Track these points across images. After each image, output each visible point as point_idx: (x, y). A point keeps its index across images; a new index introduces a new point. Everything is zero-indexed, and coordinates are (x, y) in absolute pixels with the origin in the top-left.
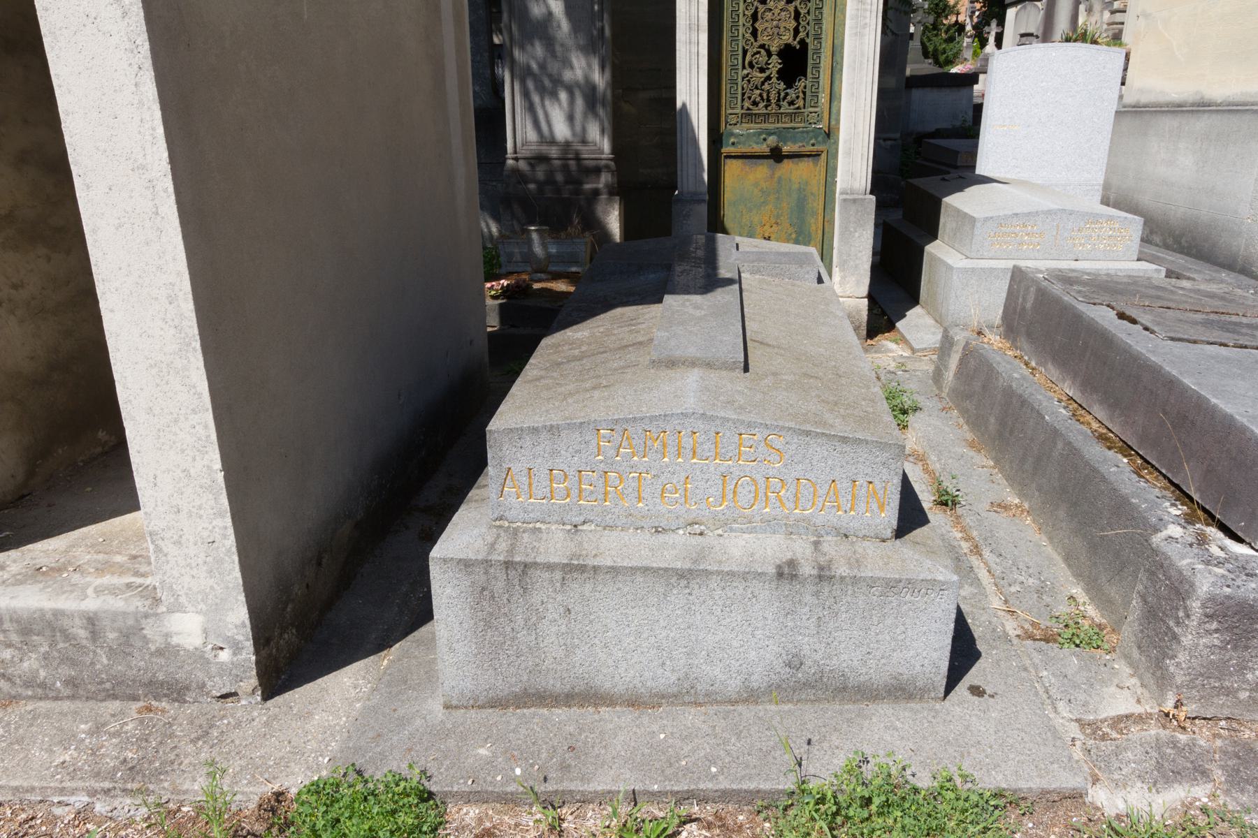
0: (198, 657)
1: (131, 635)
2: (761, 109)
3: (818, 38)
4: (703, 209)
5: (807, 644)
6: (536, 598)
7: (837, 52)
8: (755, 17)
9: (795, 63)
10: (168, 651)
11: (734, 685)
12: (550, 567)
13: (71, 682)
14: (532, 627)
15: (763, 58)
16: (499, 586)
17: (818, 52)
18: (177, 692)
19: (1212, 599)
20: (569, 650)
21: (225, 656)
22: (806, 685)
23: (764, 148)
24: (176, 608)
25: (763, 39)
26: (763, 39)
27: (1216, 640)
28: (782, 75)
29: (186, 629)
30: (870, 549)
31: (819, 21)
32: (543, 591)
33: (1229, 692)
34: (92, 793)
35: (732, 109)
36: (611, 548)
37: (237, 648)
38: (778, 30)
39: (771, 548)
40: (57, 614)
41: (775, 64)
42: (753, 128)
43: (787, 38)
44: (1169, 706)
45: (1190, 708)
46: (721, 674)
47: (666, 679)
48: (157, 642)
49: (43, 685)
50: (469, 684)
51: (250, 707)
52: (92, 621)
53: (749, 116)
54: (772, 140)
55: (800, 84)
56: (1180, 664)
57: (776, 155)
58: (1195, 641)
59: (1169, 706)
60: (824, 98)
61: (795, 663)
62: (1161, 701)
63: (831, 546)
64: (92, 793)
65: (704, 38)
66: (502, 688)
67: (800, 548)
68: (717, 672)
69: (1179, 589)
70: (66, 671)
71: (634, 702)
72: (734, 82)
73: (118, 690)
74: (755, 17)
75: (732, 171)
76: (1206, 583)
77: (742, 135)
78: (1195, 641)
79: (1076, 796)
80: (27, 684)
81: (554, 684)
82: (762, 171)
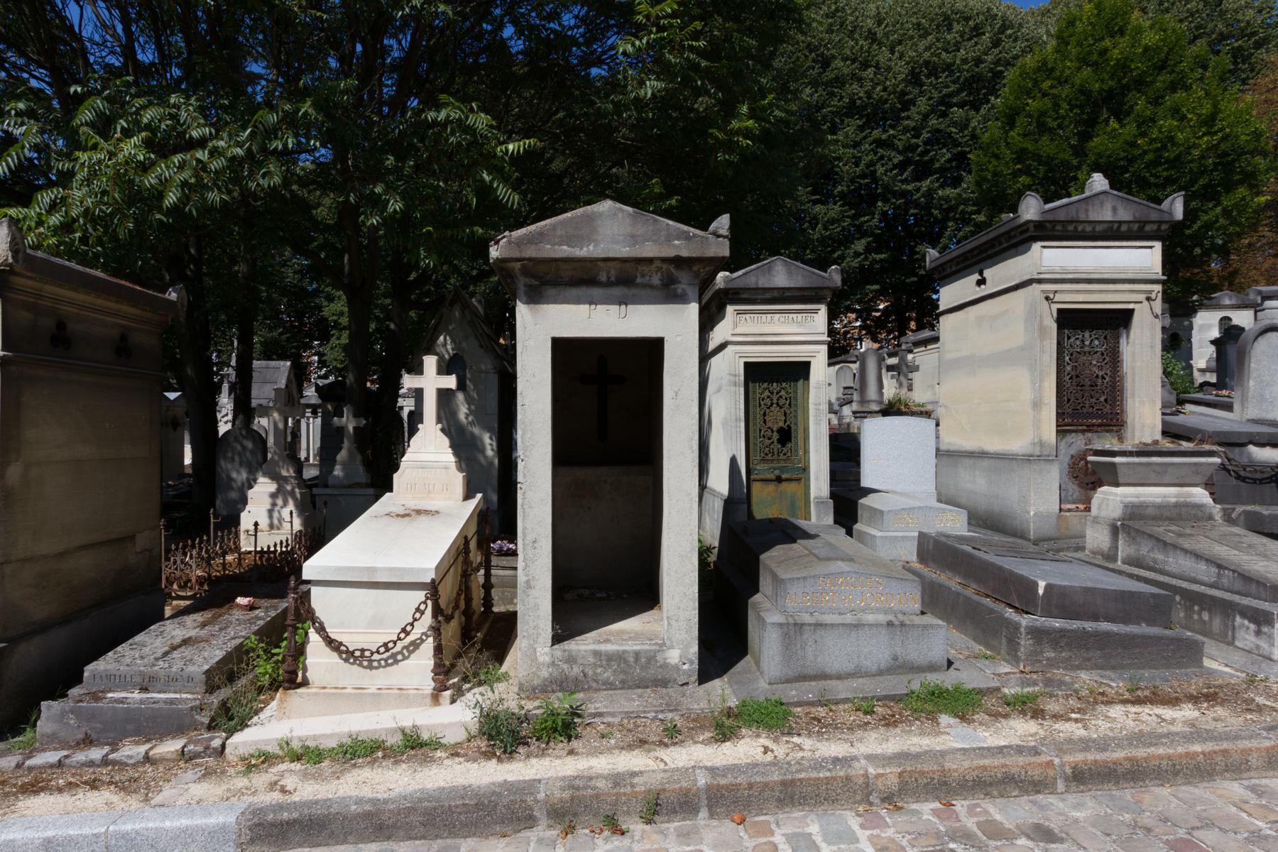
0: (677, 668)
1: (651, 658)
2: (769, 457)
3: (796, 424)
4: (745, 506)
5: (899, 650)
6: (805, 637)
7: (806, 430)
8: (764, 414)
9: (785, 436)
10: (665, 666)
11: (875, 668)
12: (810, 625)
13: (623, 682)
14: (803, 648)
15: (769, 433)
16: (792, 633)
17: (796, 431)
18: (663, 683)
19: (1027, 627)
20: (816, 657)
21: (685, 667)
22: (900, 667)
23: (772, 476)
24: (672, 647)
25: (769, 424)
26: (769, 424)
27: (1031, 642)
28: (779, 441)
29: (673, 656)
30: (914, 617)
31: (796, 417)
32: (808, 635)
33: (1040, 661)
34: (656, 712)
35: (756, 457)
36: (828, 619)
37: (692, 663)
38: (776, 420)
39: (882, 618)
40: (624, 652)
41: (776, 436)
42: (766, 466)
43: (781, 424)
44: (1022, 668)
45: (1027, 670)
46: (870, 665)
47: (849, 667)
48: (661, 662)
49: (611, 684)
50: (778, 674)
51: (693, 688)
52: (637, 655)
53: (764, 460)
54: (777, 472)
55: (789, 445)
56: (1022, 653)
57: (779, 480)
58: (1025, 643)
59: (1022, 668)
60: (801, 452)
61: (895, 658)
62: (1018, 667)
63: (900, 617)
64: (656, 712)
65: (743, 424)
66: (791, 674)
67: (891, 617)
68: (868, 663)
69: (1017, 627)
70: (622, 677)
71: (839, 677)
72: (755, 444)
73: (642, 684)
74: (764, 414)
75: (756, 487)
76: (1024, 623)
77: (761, 469)
78: (1025, 643)
79: (998, 689)
80: (604, 684)
81: (810, 672)
82: (771, 487)
